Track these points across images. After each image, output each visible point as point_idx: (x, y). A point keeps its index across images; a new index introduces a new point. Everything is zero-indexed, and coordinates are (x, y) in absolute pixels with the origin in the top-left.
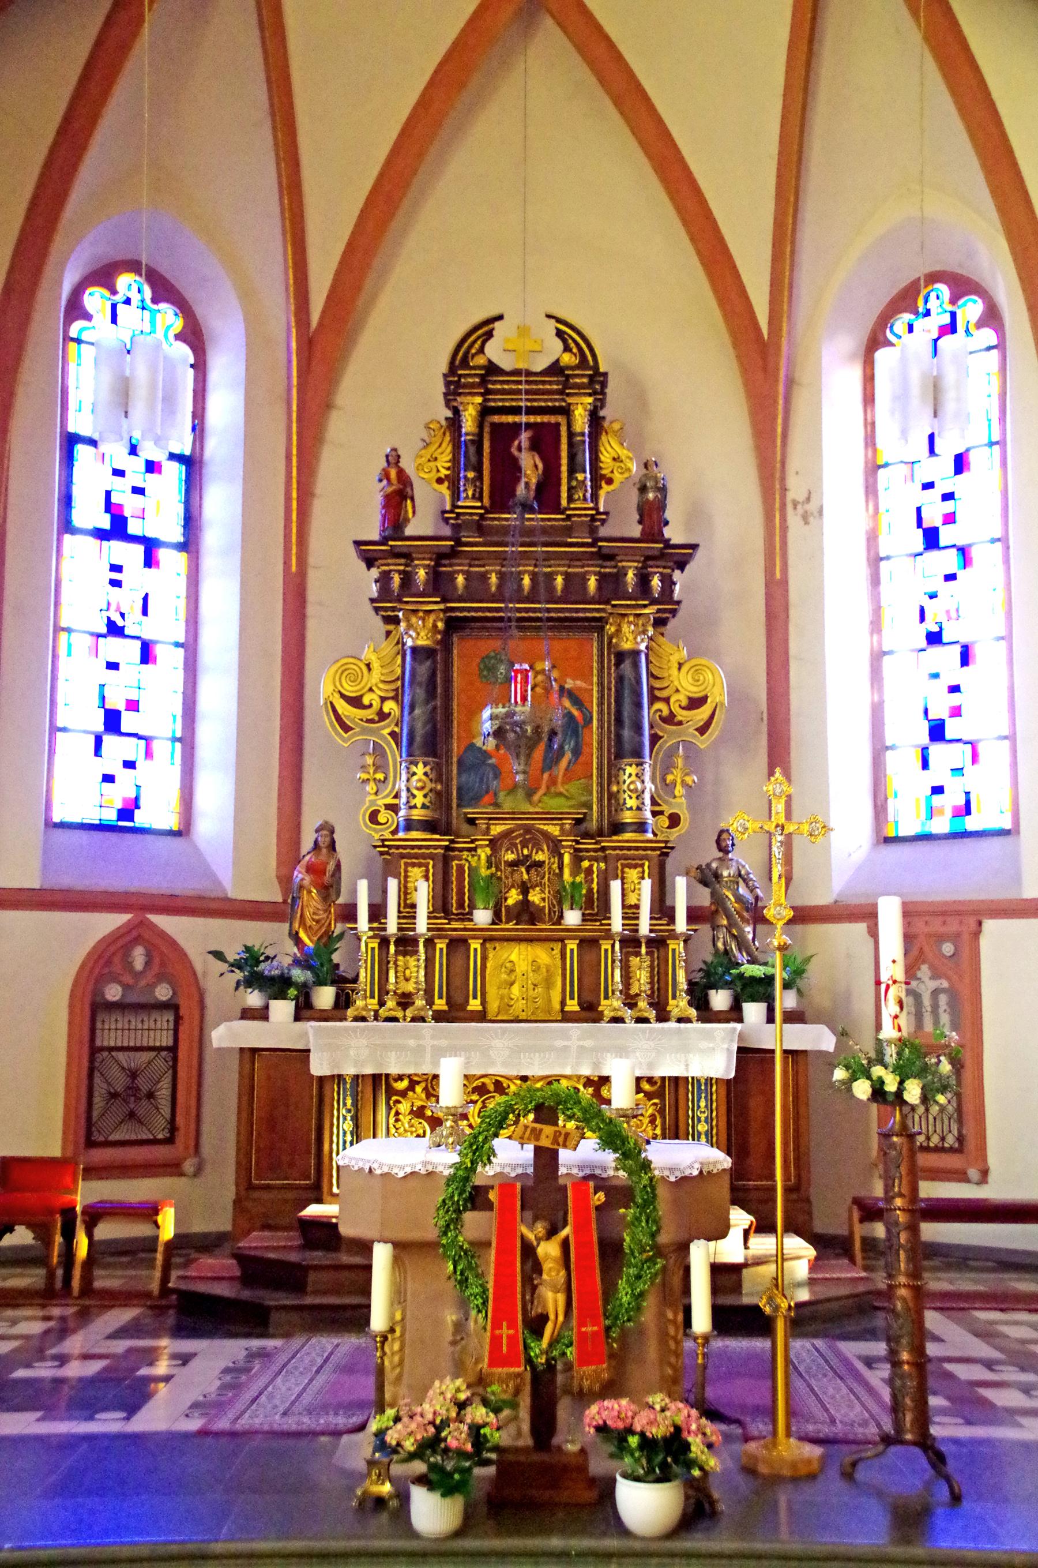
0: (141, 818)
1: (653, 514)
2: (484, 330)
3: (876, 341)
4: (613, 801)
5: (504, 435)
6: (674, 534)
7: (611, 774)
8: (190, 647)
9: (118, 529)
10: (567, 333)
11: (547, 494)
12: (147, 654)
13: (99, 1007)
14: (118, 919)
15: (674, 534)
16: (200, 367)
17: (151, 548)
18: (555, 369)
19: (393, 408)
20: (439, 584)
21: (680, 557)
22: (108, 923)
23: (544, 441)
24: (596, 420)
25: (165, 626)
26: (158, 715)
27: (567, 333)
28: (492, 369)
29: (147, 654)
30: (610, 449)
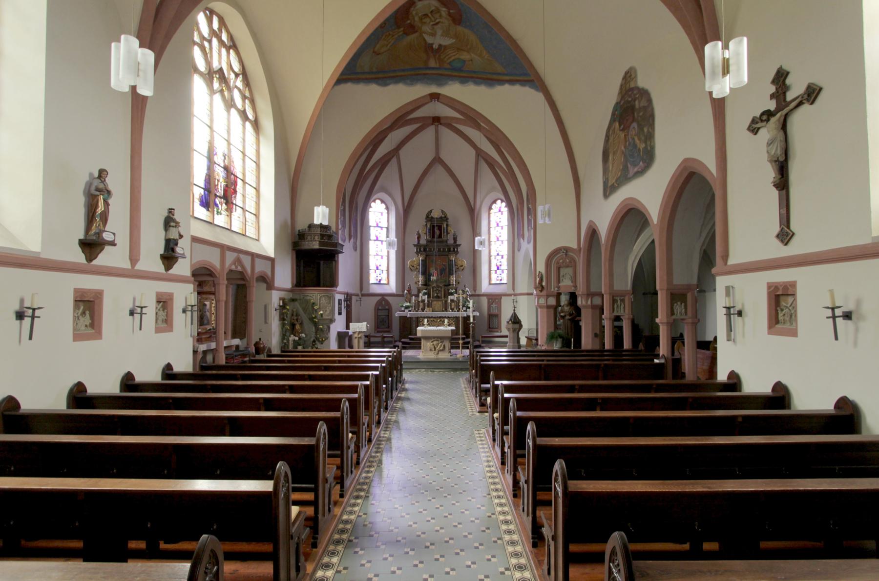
1: (455, 239)
2: (431, 211)
3: (490, 208)
4: (449, 281)
5: (433, 227)
6: (458, 243)
7: (449, 277)
9: (377, 240)
10: (443, 212)
11: (440, 236)
12: (382, 257)
13: (378, 309)
14: (379, 298)
15: (458, 243)
16: (388, 213)
17: (382, 241)
19: (418, 224)
20: (425, 250)
21: (459, 245)
22: (379, 298)
23: (440, 228)
24: (447, 225)
25: (385, 254)
26: (384, 267)
27: (443, 212)
29: (382, 257)
30: (449, 228)
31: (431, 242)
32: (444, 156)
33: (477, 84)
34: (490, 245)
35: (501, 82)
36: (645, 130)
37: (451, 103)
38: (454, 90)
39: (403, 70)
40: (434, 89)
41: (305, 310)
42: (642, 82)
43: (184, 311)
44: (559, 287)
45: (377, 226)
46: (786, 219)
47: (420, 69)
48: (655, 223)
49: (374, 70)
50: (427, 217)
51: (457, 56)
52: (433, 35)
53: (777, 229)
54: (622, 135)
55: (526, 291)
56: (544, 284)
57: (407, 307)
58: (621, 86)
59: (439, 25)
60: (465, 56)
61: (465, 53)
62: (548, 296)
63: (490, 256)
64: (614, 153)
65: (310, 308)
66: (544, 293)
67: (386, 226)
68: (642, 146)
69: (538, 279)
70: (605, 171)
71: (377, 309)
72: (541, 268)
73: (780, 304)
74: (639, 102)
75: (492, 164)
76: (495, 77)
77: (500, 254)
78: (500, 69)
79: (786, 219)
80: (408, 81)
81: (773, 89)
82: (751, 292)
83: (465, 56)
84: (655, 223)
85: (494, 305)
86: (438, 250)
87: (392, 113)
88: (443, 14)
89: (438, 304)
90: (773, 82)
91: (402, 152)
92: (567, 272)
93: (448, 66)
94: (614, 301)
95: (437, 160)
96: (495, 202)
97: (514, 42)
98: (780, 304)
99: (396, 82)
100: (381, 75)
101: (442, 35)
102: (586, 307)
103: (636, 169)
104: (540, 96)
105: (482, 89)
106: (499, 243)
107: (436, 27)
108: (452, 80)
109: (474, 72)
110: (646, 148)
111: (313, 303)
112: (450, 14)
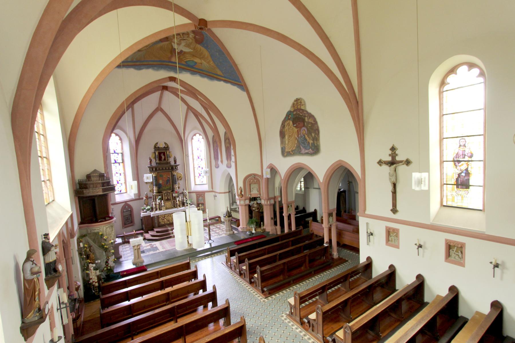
0: (122, 192)
2: (157, 143)
8: (125, 173)
9: (116, 162)
10: (165, 143)
11: (165, 159)
12: (120, 175)
16: (122, 143)
17: (119, 163)
18: (165, 147)
27: (165, 143)
28: (158, 147)
29: (120, 175)
31: (159, 164)
32: (163, 107)
33: (202, 76)
34: (193, 161)
35: (219, 80)
36: (313, 135)
37: (183, 84)
38: (186, 77)
39: (154, 61)
40: (172, 74)
41: (94, 241)
42: (310, 108)
43: (58, 310)
44: (251, 194)
45: (115, 153)
46: (394, 205)
47: (164, 61)
48: (321, 181)
49: (135, 60)
50: (155, 147)
51: (192, 59)
52: (179, 44)
53: (391, 208)
54: (296, 130)
55: (223, 191)
56: (243, 193)
57: (148, 210)
58: (294, 104)
59: (185, 41)
60: (197, 60)
61: (198, 59)
62: (245, 200)
63: (194, 168)
64: (289, 136)
65: (99, 238)
66: (243, 198)
67: (121, 152)
68: (311, 142)
69: (239, 191)
70: (282, 142)
71: (122, 212)
72: (241, 184)
73: (391, 236)
74: (308, 120)
75: (197, 115)
76: (215, 76)
77: (201, 166)
78: (219, 73)
79: (394, 205)
80: (156, 68)
81: (390, 152)
82: (379, 229)
83: (197, 60)
84: (321, 181)
85: (201, 198)
86: (164, 170)
87: (142, 88)
88: (191, 36)
89: (169, 204)
90: (391, 149)
91: (136, 106)
92: (254, 187)
93: (185, 63)
94: (288, 207)
95: (159, 109)
96: (195, 135)
97: (236, 65)
98: (391, 236)
99: (148, 68)
100: (138, 63)
101: (185, 46)
102: (266, 205)
103: (307, 151)
104: (245, 94)
105: (205, 80)
106: (200, 160)
107: (182, 41)
108: (185, 71)
109: (201, 70)
110: (313, 143)
111: (102, 235)
112: (195, 38)
